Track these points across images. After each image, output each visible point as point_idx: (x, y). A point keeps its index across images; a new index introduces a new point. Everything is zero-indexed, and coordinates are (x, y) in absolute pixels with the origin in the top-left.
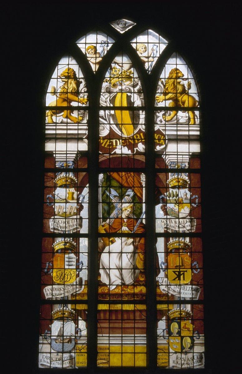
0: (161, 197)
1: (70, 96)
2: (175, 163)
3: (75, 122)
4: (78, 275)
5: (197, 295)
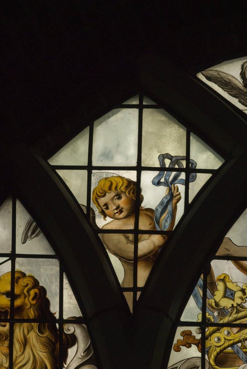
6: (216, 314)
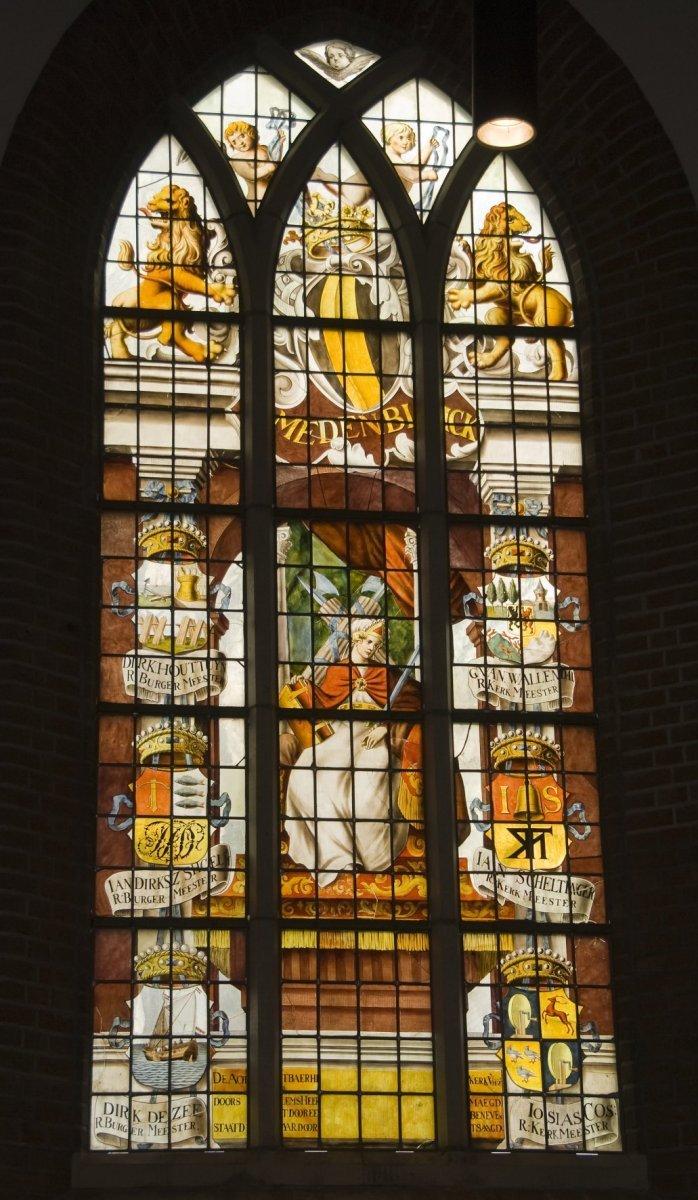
0: (466, 599)
1: (182, 277)
2: (509, 499)
3: (200, 358)
4: (214, 839)
5: (584, 906)
6: (312, 220)
